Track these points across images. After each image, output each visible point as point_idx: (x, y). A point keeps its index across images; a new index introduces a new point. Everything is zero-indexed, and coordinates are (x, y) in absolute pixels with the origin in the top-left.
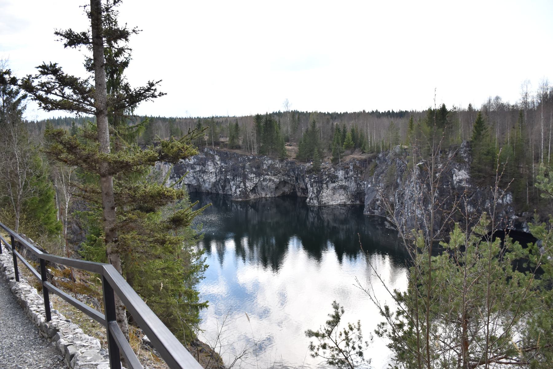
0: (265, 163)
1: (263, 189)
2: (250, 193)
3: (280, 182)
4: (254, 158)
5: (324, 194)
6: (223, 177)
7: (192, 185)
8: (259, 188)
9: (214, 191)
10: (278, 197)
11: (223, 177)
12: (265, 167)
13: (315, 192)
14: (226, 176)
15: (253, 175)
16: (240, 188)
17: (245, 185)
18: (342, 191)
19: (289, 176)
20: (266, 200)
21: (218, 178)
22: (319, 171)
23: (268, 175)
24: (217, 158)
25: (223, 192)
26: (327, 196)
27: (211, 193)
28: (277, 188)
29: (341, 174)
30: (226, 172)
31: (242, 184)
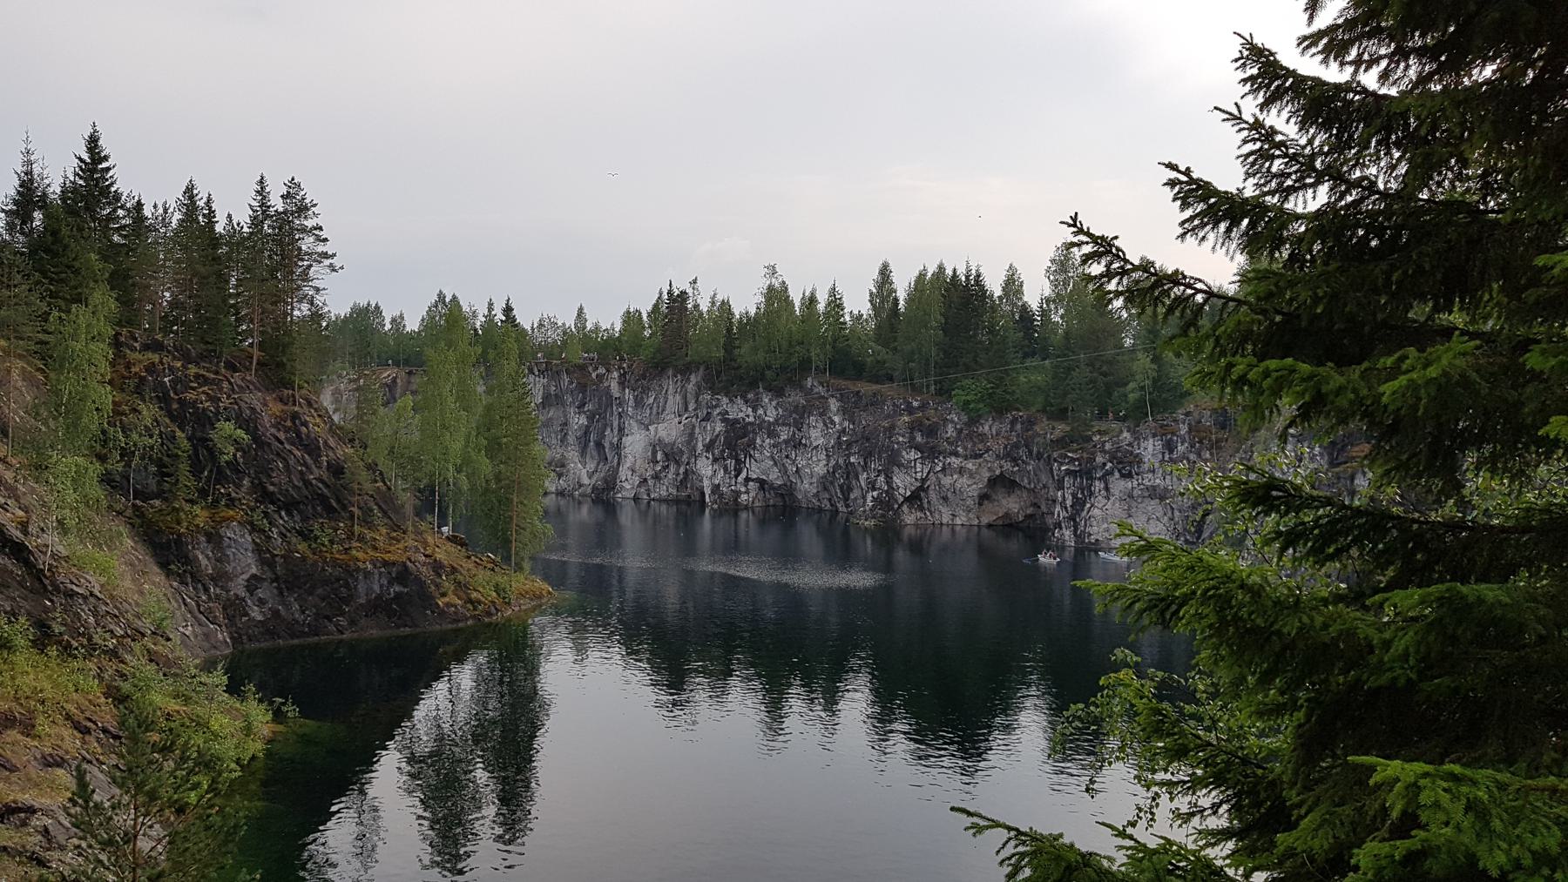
0: (952, 421)
1: (945, 499)
2: (905, 508)
3: (994, 482)
4: (923, 407)
5: (1096, 512)
6: (841, 461)
7: (772, 487)
8: (933, 495)
9: (826, 505)
10: (989, 526)
11: (841, 461)
12: (950, 431)
13: (1069, 503)
14: (848, 456)
15: (913, 455)
16: (874, 489)
17: (889, 480)
18: (1153, 506)
19: (1015, 460)
20: (953, 531)
21: (833, 462)
22: (1089, 439)
23: (956, 454)
24: (834, 405)
25: (847, 506)
26: (1104, 520)
27: (820, 510)
28: (983, 498)
29: (1150, 449)
30: (849, 444)
31: (882, 478)
